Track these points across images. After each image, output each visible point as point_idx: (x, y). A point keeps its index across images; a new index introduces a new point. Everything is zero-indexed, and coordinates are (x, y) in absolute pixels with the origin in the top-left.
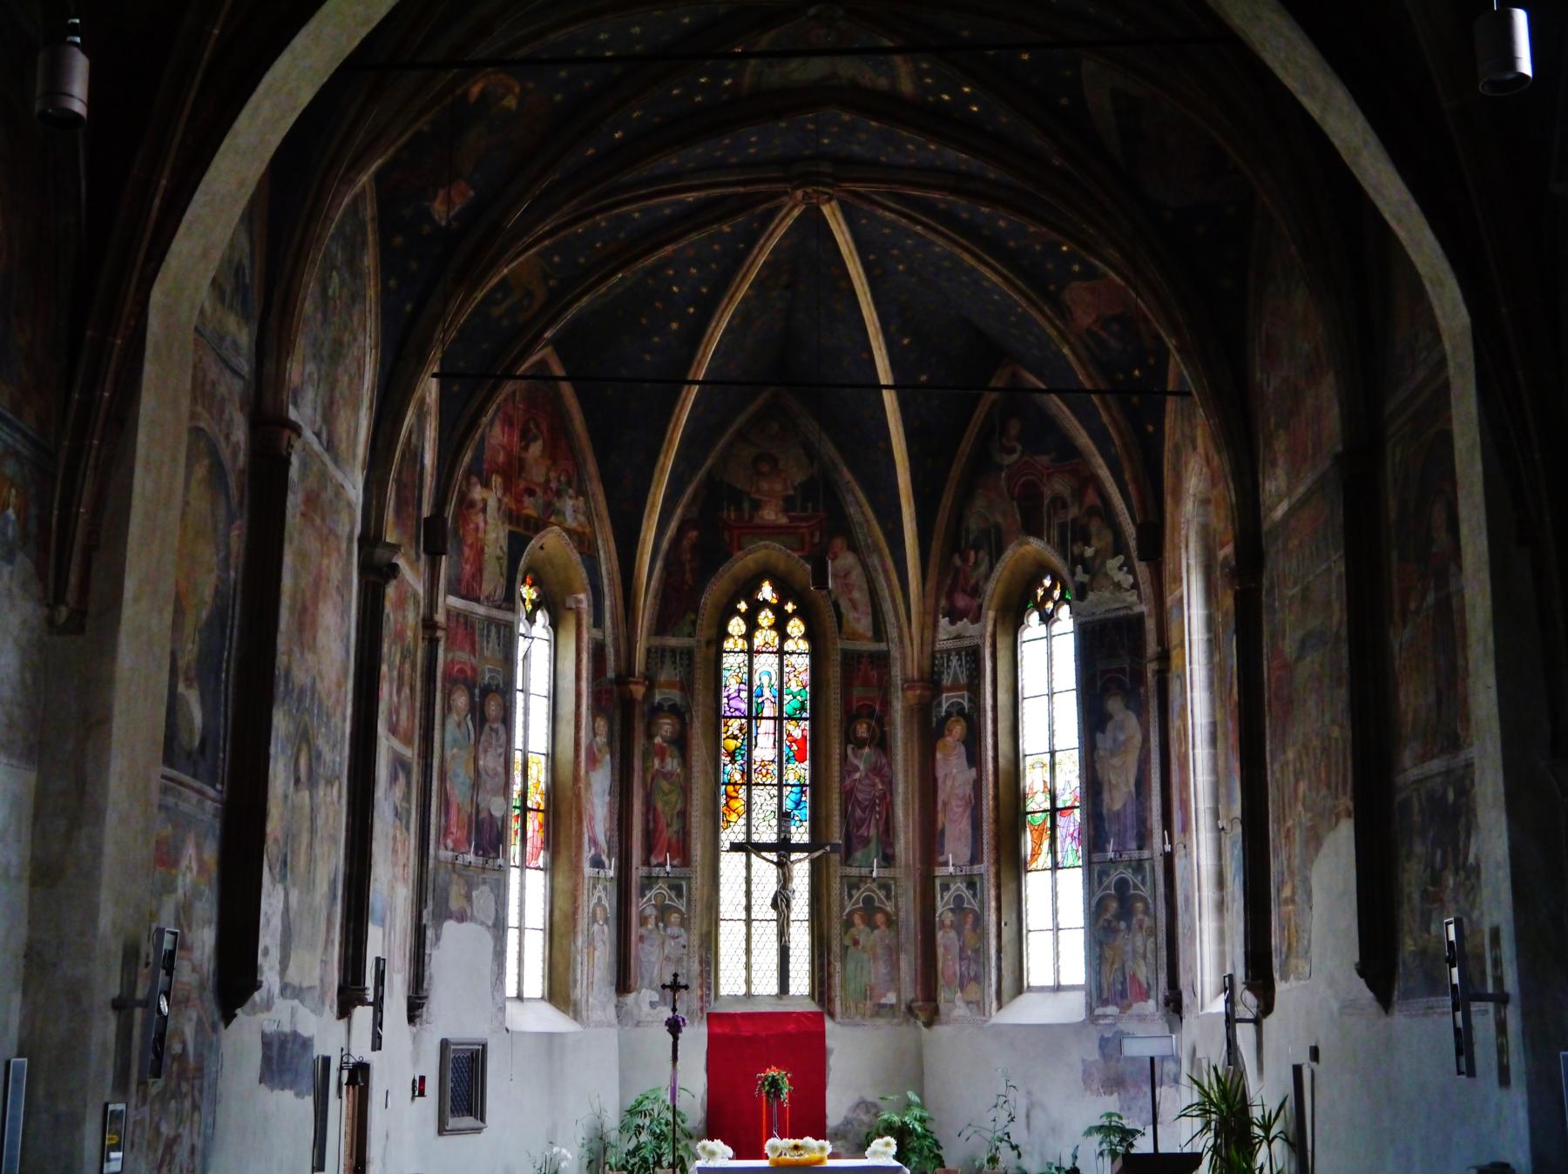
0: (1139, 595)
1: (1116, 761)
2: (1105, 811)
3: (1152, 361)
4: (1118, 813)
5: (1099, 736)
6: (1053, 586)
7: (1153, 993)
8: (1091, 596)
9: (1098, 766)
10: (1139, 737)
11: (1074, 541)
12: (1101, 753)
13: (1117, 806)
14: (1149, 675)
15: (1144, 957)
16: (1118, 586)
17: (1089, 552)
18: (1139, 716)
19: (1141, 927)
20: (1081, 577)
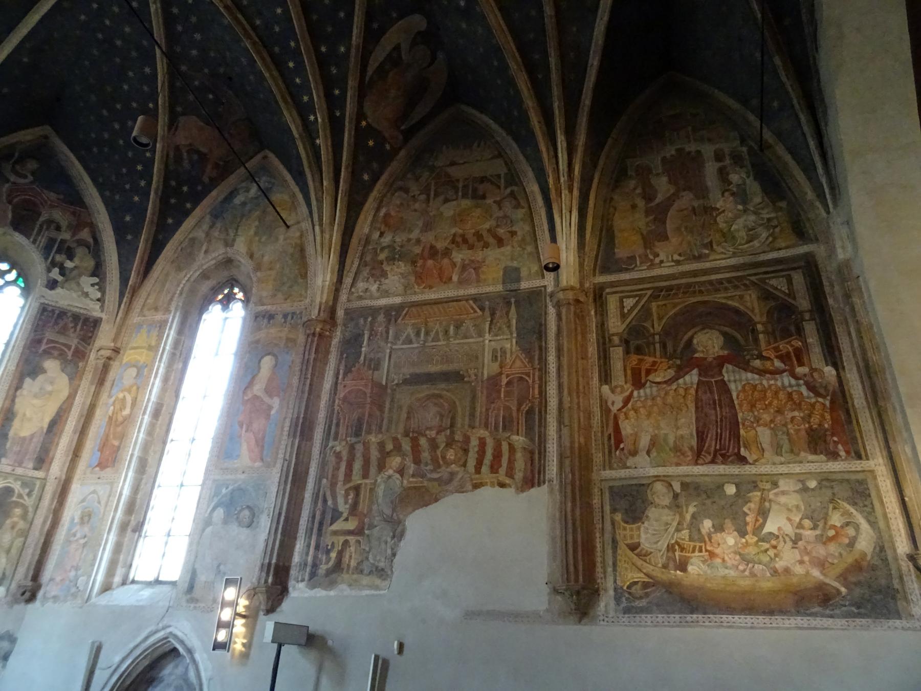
0: (102, 307)
1: (35, 401)
2: (11, 434)
3: (199, 188)
4: (24, 439)
5: (28, 380)
6: (9, 271)
7: (6, 582)
8: (59, 290)
9: (17, 400)
10: (65, 393)
11: (59, 251)
12: (25, 392)
13: (25, 433)
14: (92, 356)
15: (8, 551)
16: (86, 295)
17: (69, 264)
18: (71, 379)
19: (13, 528)
20: (55, 273)
